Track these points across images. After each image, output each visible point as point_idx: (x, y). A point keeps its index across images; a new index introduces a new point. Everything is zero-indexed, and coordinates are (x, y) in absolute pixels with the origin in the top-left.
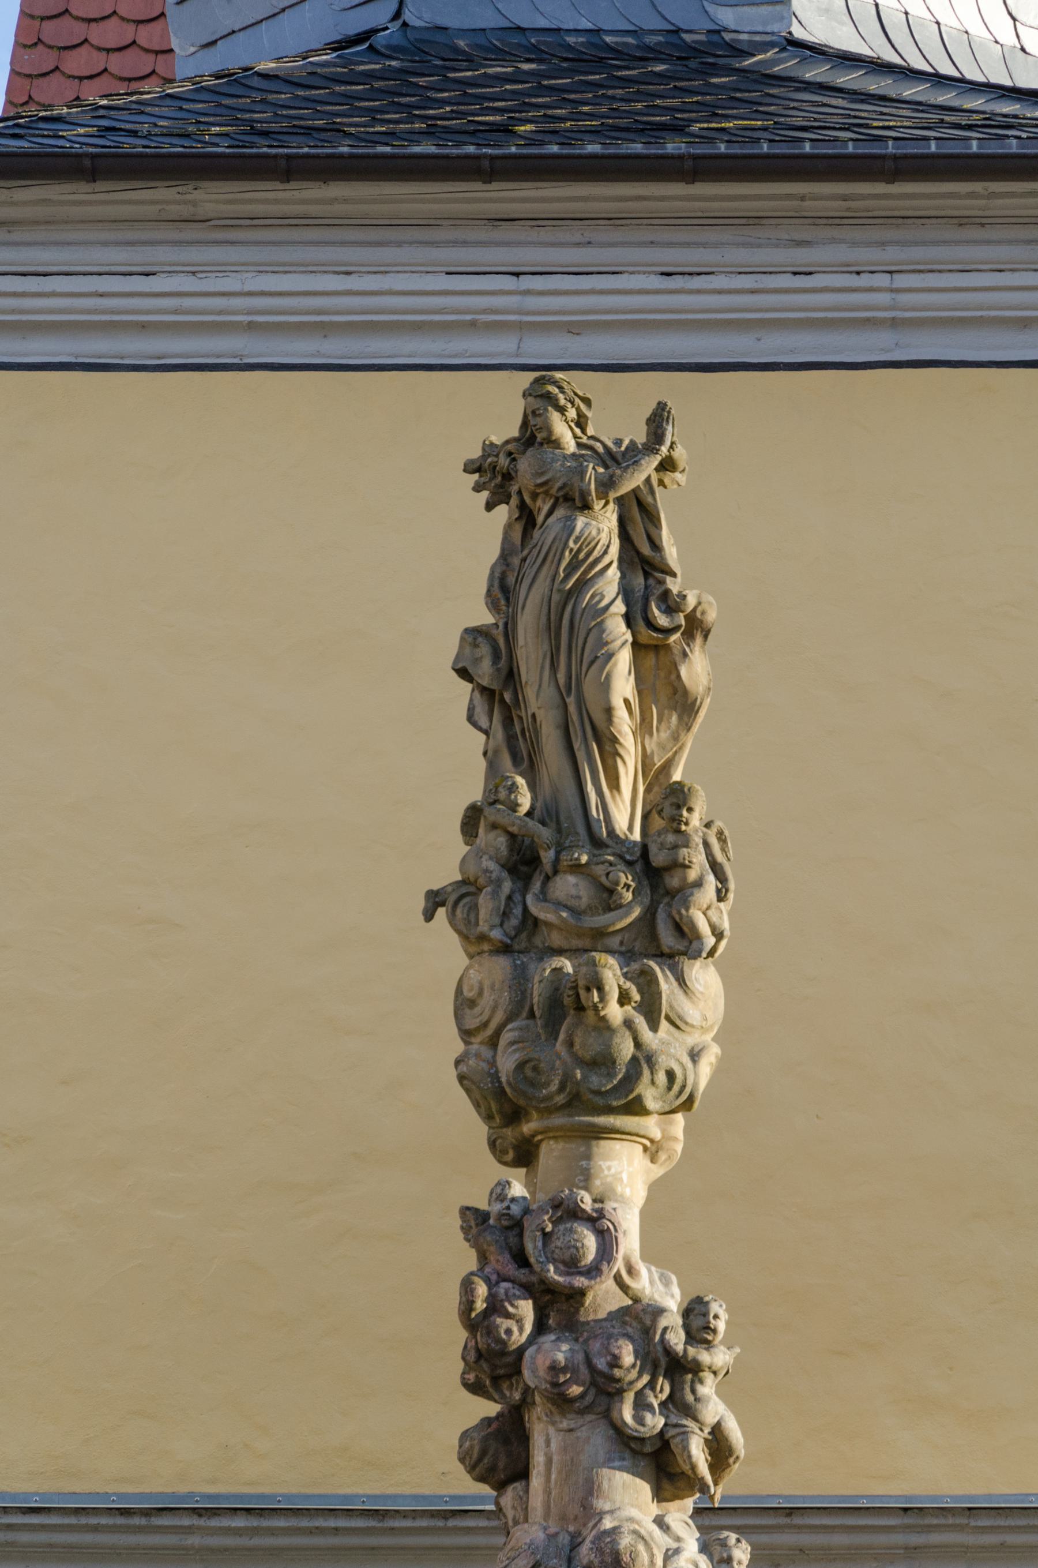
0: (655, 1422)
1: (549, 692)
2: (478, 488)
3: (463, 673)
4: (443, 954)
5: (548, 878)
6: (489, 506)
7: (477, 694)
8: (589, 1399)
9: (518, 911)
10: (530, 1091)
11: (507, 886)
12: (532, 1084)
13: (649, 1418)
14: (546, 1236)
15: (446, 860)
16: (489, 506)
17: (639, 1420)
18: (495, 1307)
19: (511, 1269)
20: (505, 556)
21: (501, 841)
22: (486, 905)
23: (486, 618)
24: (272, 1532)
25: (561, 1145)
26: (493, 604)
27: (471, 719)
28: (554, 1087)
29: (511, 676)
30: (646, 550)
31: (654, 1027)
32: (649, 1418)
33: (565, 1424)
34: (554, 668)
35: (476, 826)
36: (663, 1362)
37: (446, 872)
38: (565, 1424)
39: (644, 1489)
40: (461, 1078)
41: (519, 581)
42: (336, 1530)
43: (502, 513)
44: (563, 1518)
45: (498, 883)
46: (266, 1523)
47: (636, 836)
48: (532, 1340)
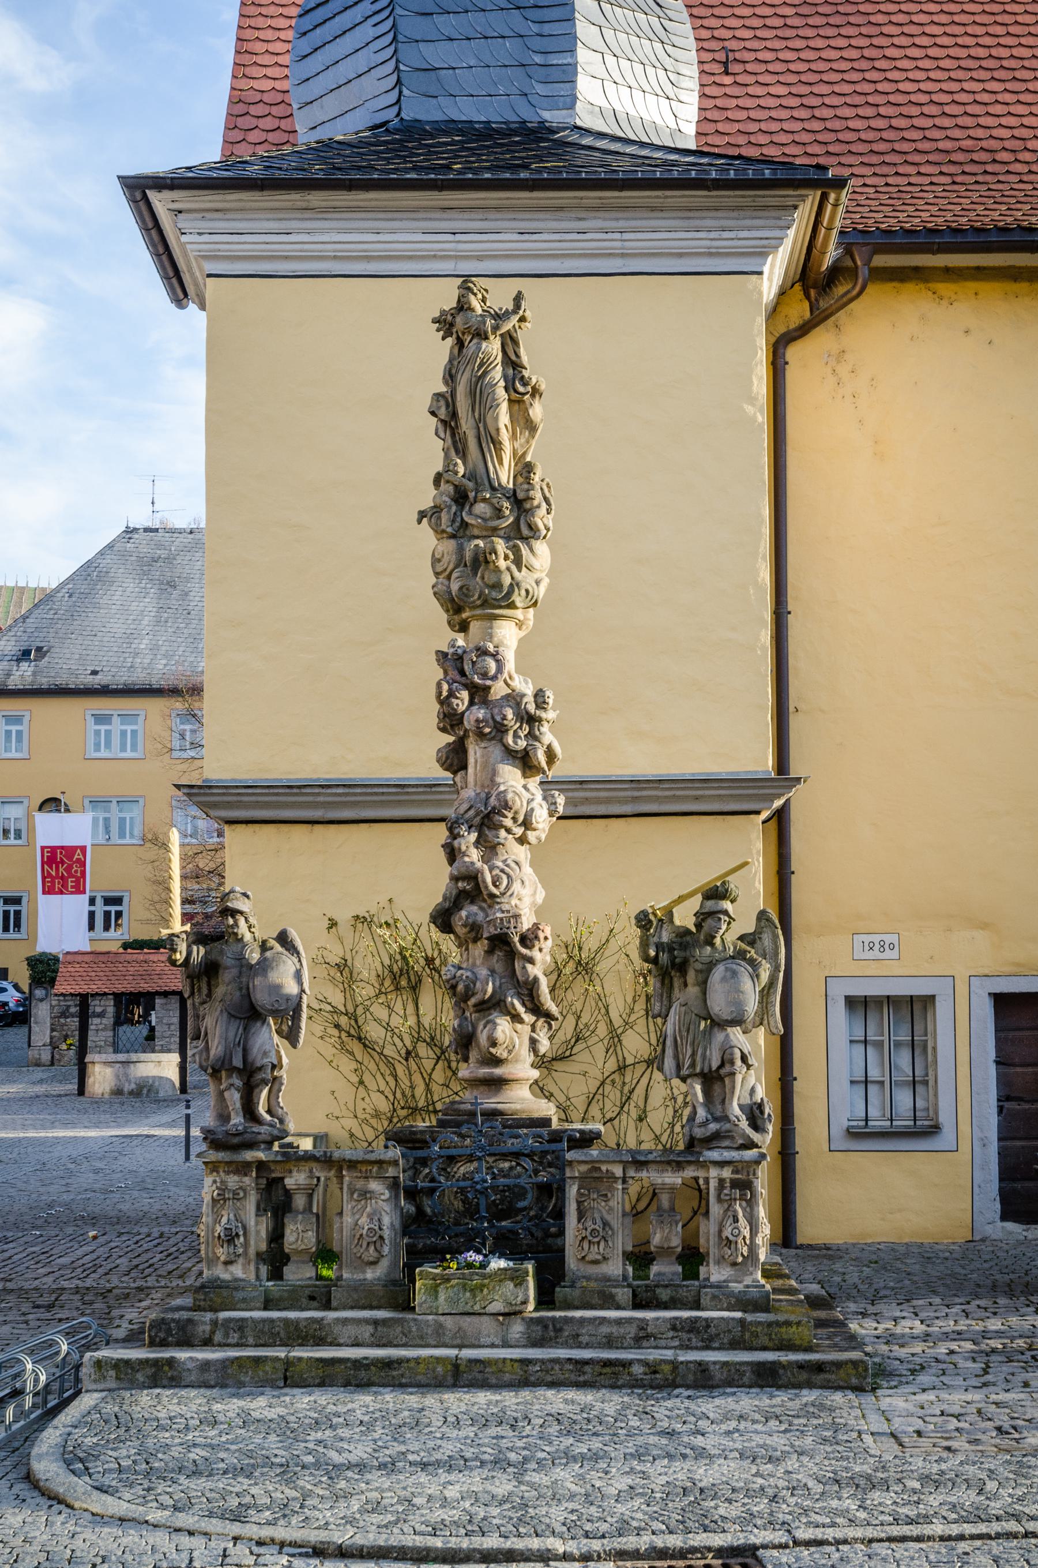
0: (522, 744)
1: (471, 421)
2: (438, 330)
3: (433, 413)
4: (426, 540)
5: (472, 505)
6: (443, 339)
7: (440, 425)
8: (493, 734)
9: (459, 519)
10: (465, 599)
11: (454, 508)
12: (466, 596)
13: (519, 741)
14: (474, 663)
15: (427, 497)
16: (443, 339)
17: (516, 743)
18: (451, 694)
19: (458, 678)
20: (450, 361)
21: (451, 488)
22: (445, 517)
23: (443, 389)
24: (355, 794)
25: (479, 623)
26: (446, 383)
27: (436, 434)
28: (476, 597)
29: (454, 415)
30: (513, 358)
31: (520, 571)
32: (519, 741)
33: (483, 745)
34: (473, 411)
35: (440, 482)
36: (526, 717)
37: (427, 503)
38: (483, 745)
39: (518, 773)
40: (435, 594)
41: (457, 372)
42: (383, 793)
43: (450, 341)
44: (483, 786)
45: (450, 507)
46: (351, 791)
47: (511, 486)
48: (468, 709)
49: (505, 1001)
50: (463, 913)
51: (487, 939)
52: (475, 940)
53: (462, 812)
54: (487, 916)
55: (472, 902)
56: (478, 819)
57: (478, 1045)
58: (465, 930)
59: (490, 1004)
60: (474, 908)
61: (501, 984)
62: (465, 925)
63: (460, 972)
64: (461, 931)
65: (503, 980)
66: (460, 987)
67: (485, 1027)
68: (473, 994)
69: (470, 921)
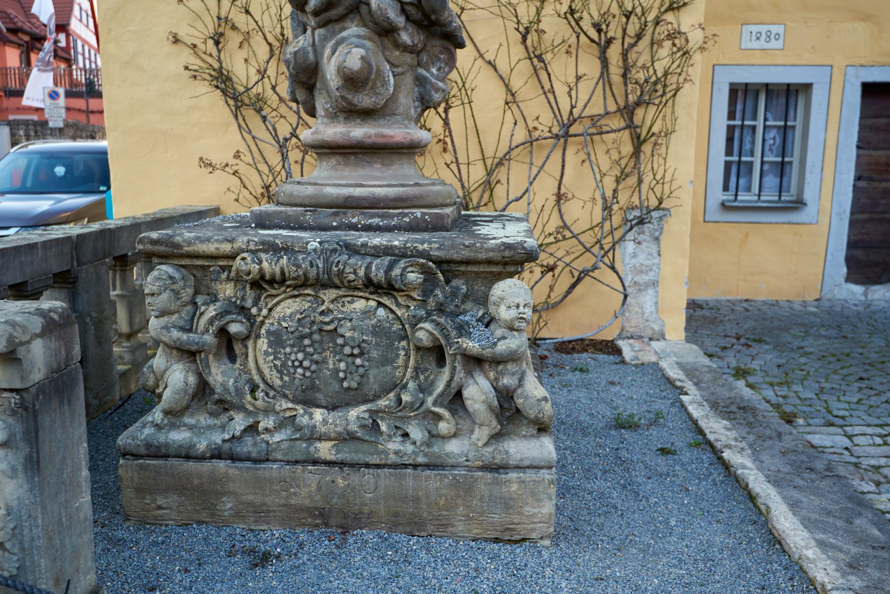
57: (326, 86)
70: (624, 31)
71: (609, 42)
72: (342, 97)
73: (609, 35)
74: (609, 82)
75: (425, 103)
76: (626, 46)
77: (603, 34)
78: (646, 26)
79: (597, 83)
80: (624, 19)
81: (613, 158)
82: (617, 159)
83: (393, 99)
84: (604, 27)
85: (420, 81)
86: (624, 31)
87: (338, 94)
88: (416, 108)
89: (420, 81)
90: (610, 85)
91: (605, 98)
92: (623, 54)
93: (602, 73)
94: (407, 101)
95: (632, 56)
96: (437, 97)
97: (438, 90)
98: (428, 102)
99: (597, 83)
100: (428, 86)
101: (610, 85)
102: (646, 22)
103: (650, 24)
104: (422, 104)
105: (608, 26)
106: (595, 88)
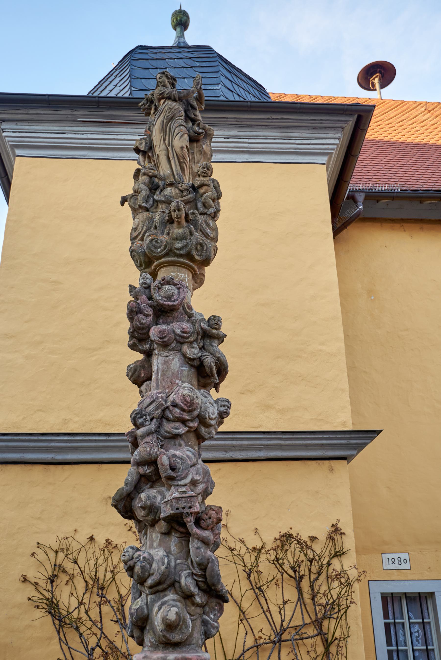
49: (179, 582)
50: (143, 496)
51: (165, 519)
52: (153, 523)
53: (145, 405)
54: (164, 497)
55: (151, 487)
56: (159, 411)
57: (153, 629)
58: (143, 513)
59: (165, 586)
60: (153, 492)
61: (176, 565)
62: (143, 508)
63: (138, 553)
64: (140, 514)
65: (178, 561)
66: (137, 569)
67: (160, 609)
68: (150, 575)
69: (148, 503)
70: (310, 570)
71: (301, 577)
72: (164, 636)
73: (301, 574)
74: (304, 603)
75: (207, 635)
76: (312, 580)
77: (297, 573)
78: (323, 567)
79: (297, 605)
80: (309, 563)
81: (312, 656)
82: (315, 657)
83: (191, 635)
84: (297, 568)
85: (205, 623)
86: (310, 570)
87: (161, 634)
88: (202, 639)
89: (205, 623)
90: (305, 605)
91: (302, 615)
92: (310, 586)
93: (299, 597)
94: (197, 636)
95: (316, 587)
96: (213, 631)
97: (214, 627)
98: (208, 635)
99: (297, 605)
100: (209, 626)
101: (305, 605)
102: (322, 565)
103: (325, 566)
104: (206, 636)
105: (299, 567)
106: (296, 607)
